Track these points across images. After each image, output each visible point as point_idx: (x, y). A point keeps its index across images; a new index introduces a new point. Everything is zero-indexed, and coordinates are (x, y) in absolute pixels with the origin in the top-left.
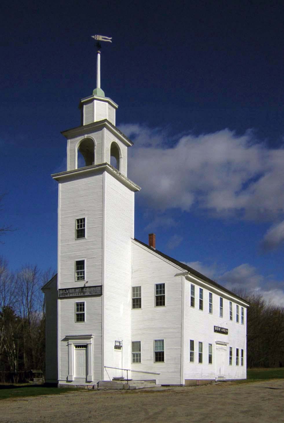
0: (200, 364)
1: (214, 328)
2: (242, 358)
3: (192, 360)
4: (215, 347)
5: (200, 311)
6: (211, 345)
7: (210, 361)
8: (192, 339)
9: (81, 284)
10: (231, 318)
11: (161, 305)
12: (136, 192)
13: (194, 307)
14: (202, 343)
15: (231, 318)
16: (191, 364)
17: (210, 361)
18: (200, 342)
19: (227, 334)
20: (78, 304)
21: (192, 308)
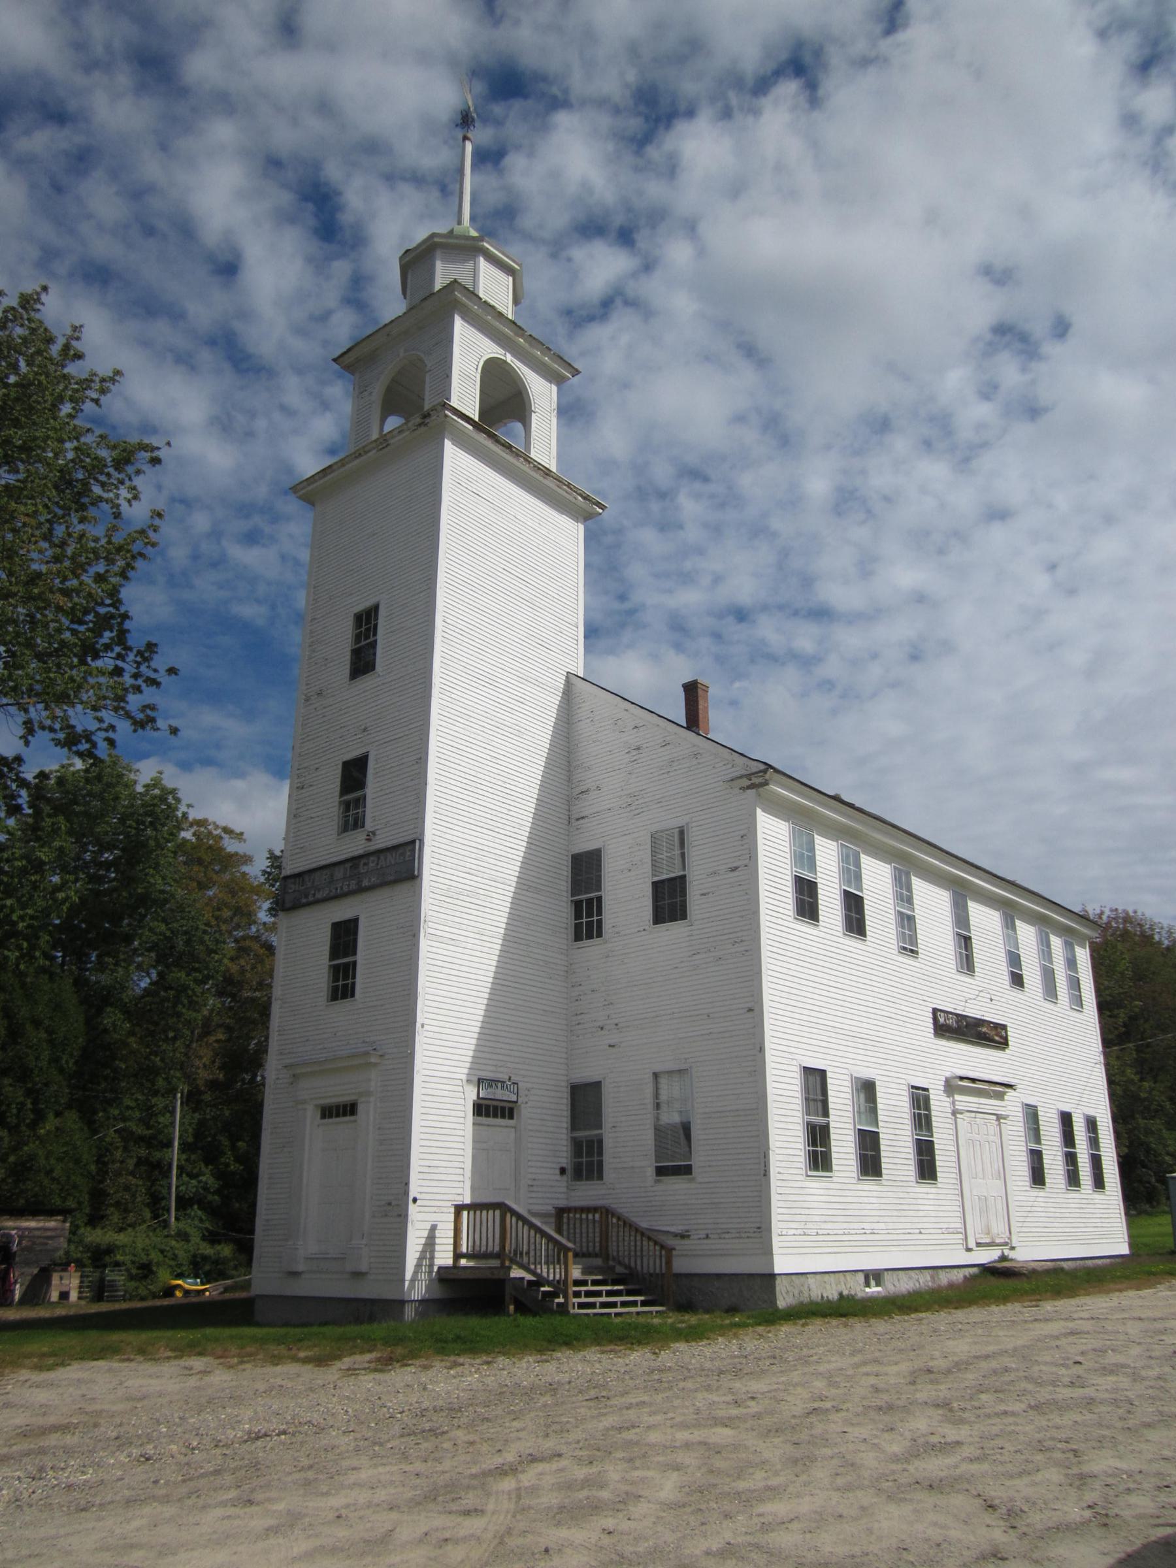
0: (870, 1187)
1: (935, 1019)
2: (1035, 1147)
3: (820, 1160)
4: (939, 1104)
5: (852, 944)
6: (822, 1073)
7: (927, 1169)
8: (866, 1073)
9: (355, 844)
10: (1017, 980)
11: (673, 918)
12: (589, 523)
13: (818, 921)
14: (822, 1073)
15: (1017, 980)
16: (817, 1187)
17: (927, 1169)
18: (808, 1071)
19: (1003, 1049)
20: (336, 926)
21: (804, 928)
